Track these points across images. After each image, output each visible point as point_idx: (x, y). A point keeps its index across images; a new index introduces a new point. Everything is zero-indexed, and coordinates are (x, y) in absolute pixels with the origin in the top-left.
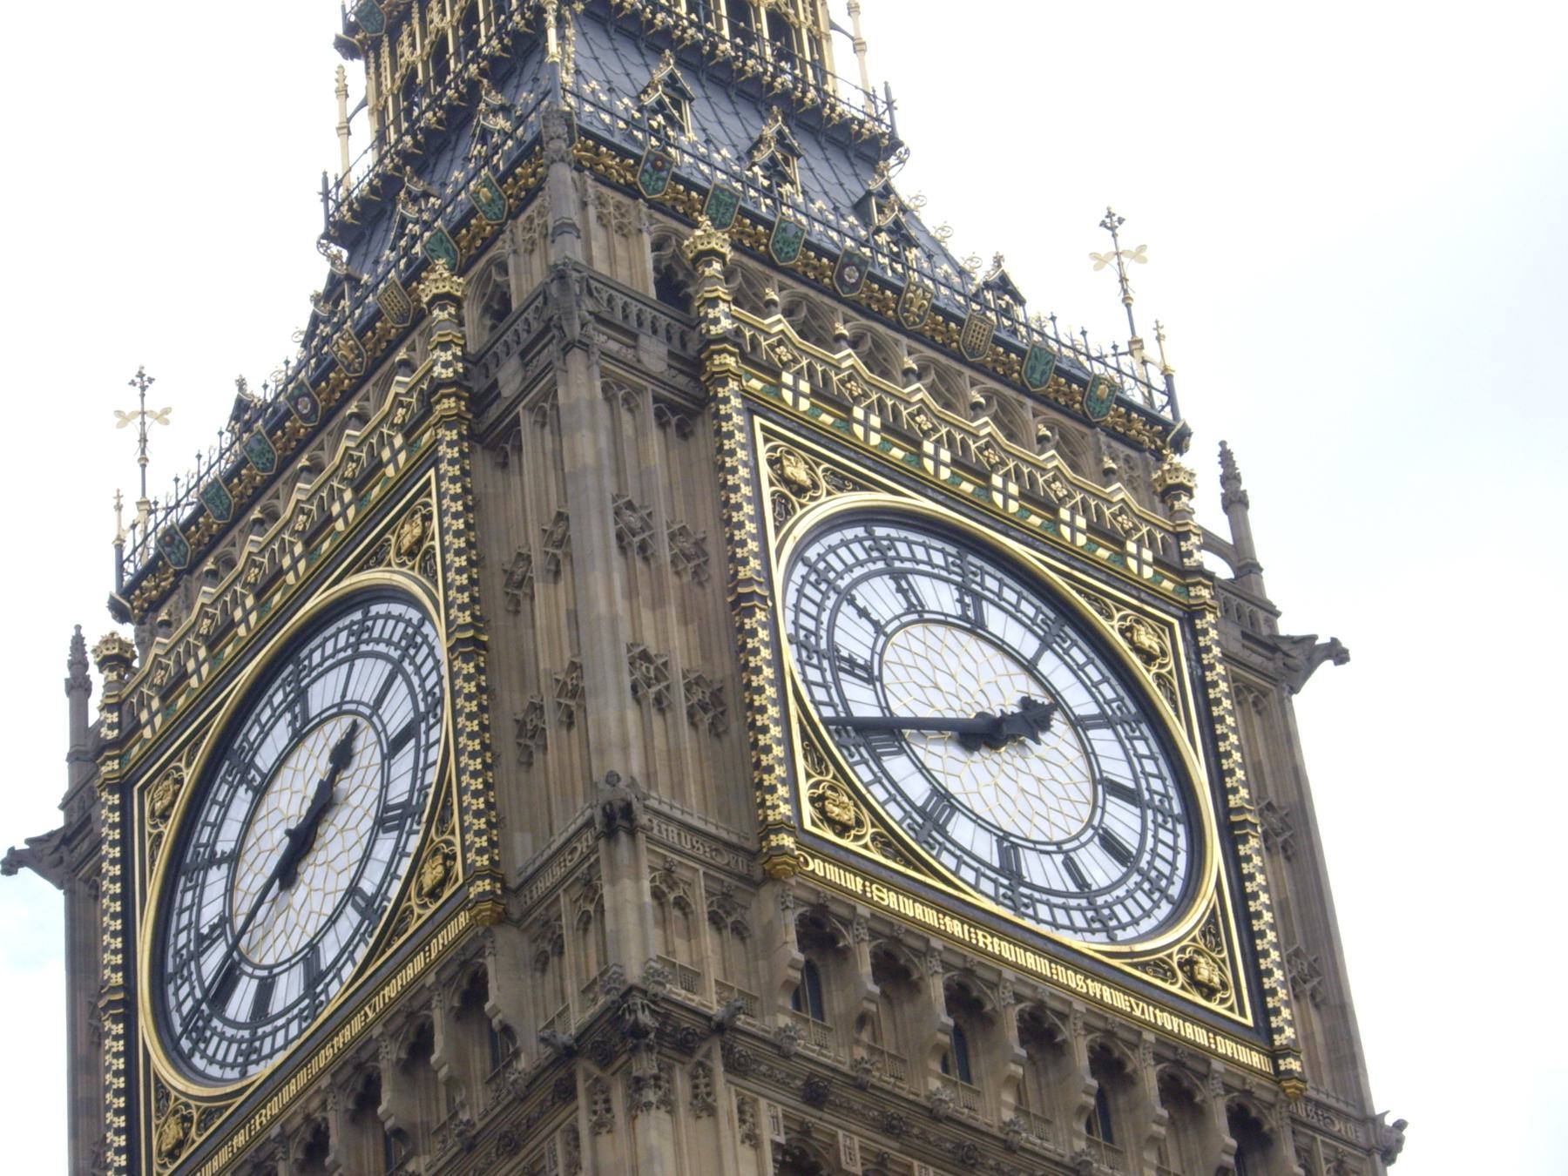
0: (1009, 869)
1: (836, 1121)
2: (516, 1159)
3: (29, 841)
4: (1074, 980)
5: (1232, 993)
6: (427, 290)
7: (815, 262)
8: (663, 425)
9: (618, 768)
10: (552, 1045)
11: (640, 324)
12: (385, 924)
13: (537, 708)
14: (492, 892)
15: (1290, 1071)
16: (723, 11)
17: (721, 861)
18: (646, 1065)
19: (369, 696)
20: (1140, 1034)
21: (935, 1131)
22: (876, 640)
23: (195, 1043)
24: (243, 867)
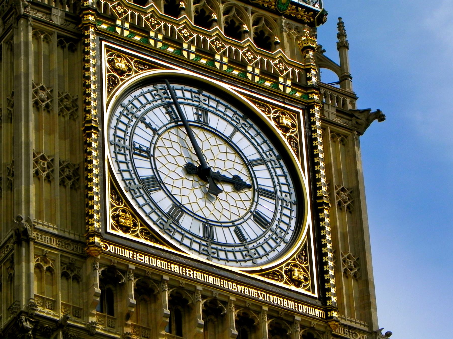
8: (63, 48)
15: (332, 317)
17: (69, 249)
20: (261, 307)
22: (153, 138)
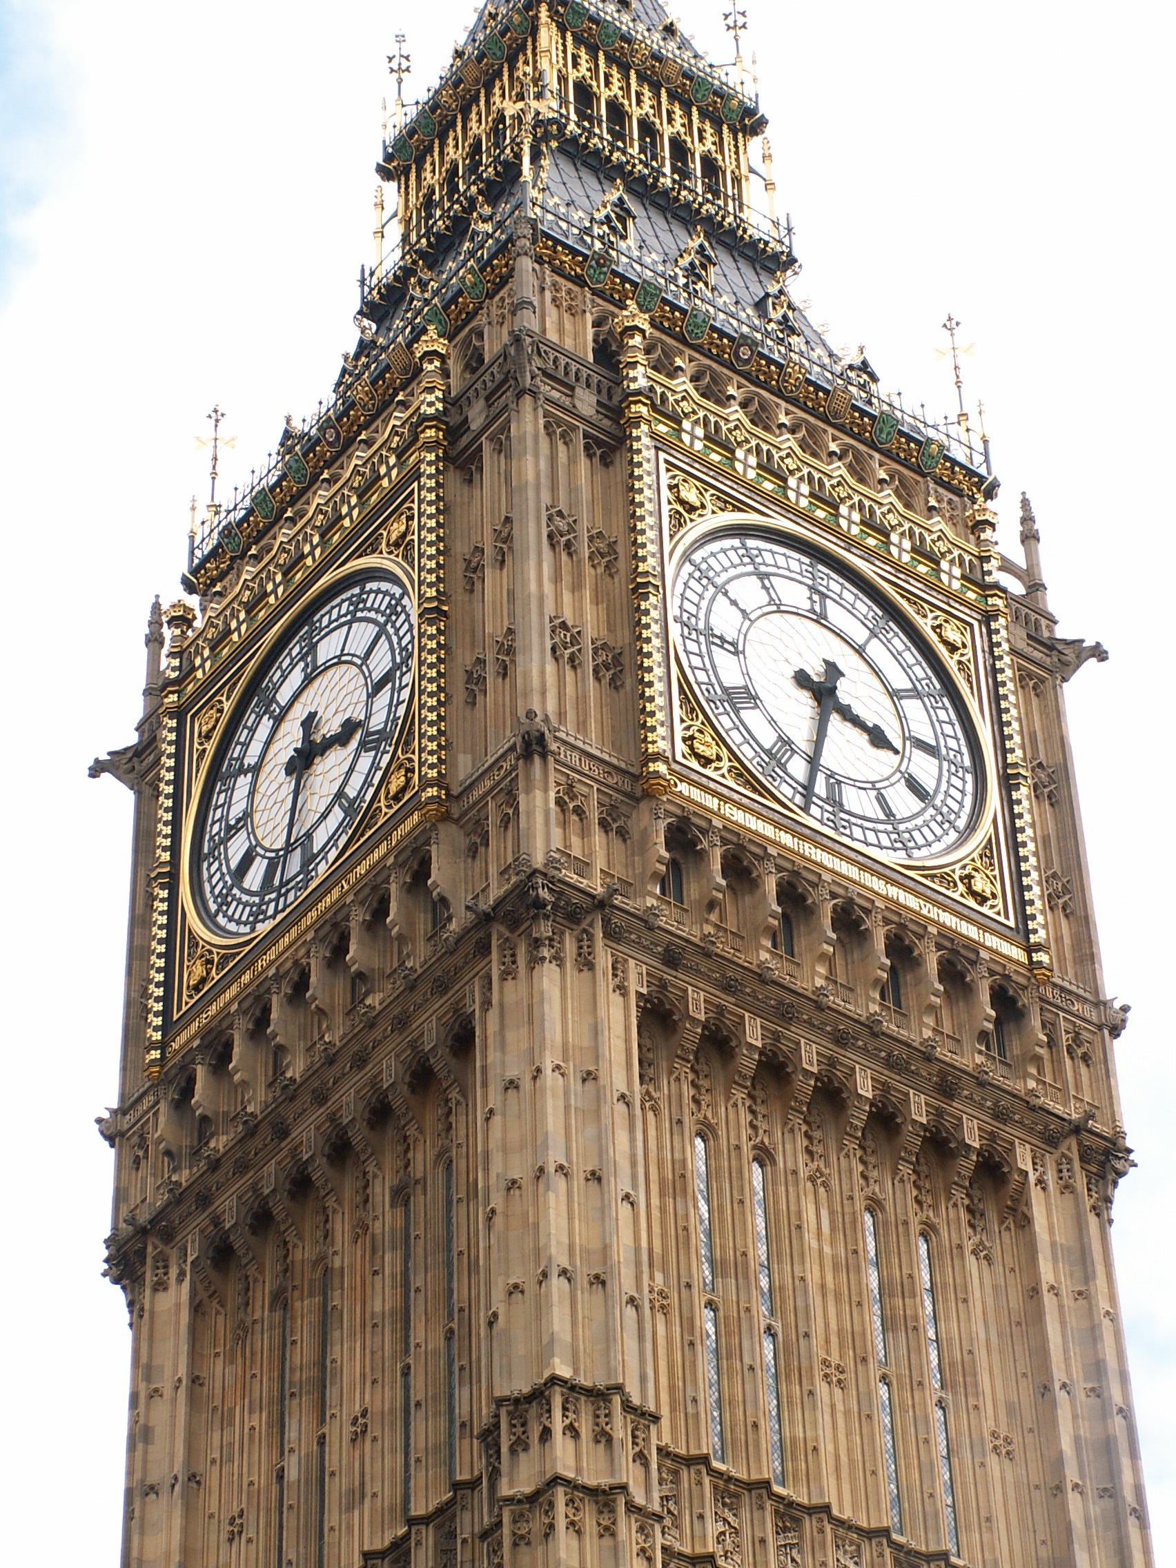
1: (687, 979)
2: (445, 998)
3: (109, 754)
4: (878, 885)
5: (999, 901)
6: (420, 349)
7: (718, 342)
8: (590, 456)
9: (537, 708)
10: (475, 912)
11: (577, 380)
12: (361, 819)
13: (481, 662)
14: (439, 797)
15: (1040, 962)
16: (667, 154)
17: (611, 781)
18: (544, 929)
19: (361, 651)
23: (220, 906)
24: (262, 776)
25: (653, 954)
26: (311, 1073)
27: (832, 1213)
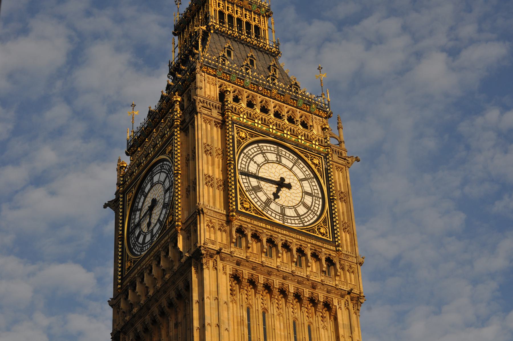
0: (283, 214)
19: (163, 180)
21: (263, 269)
25: (234, 263)
26: (154, 294)
27: (284, 323)
